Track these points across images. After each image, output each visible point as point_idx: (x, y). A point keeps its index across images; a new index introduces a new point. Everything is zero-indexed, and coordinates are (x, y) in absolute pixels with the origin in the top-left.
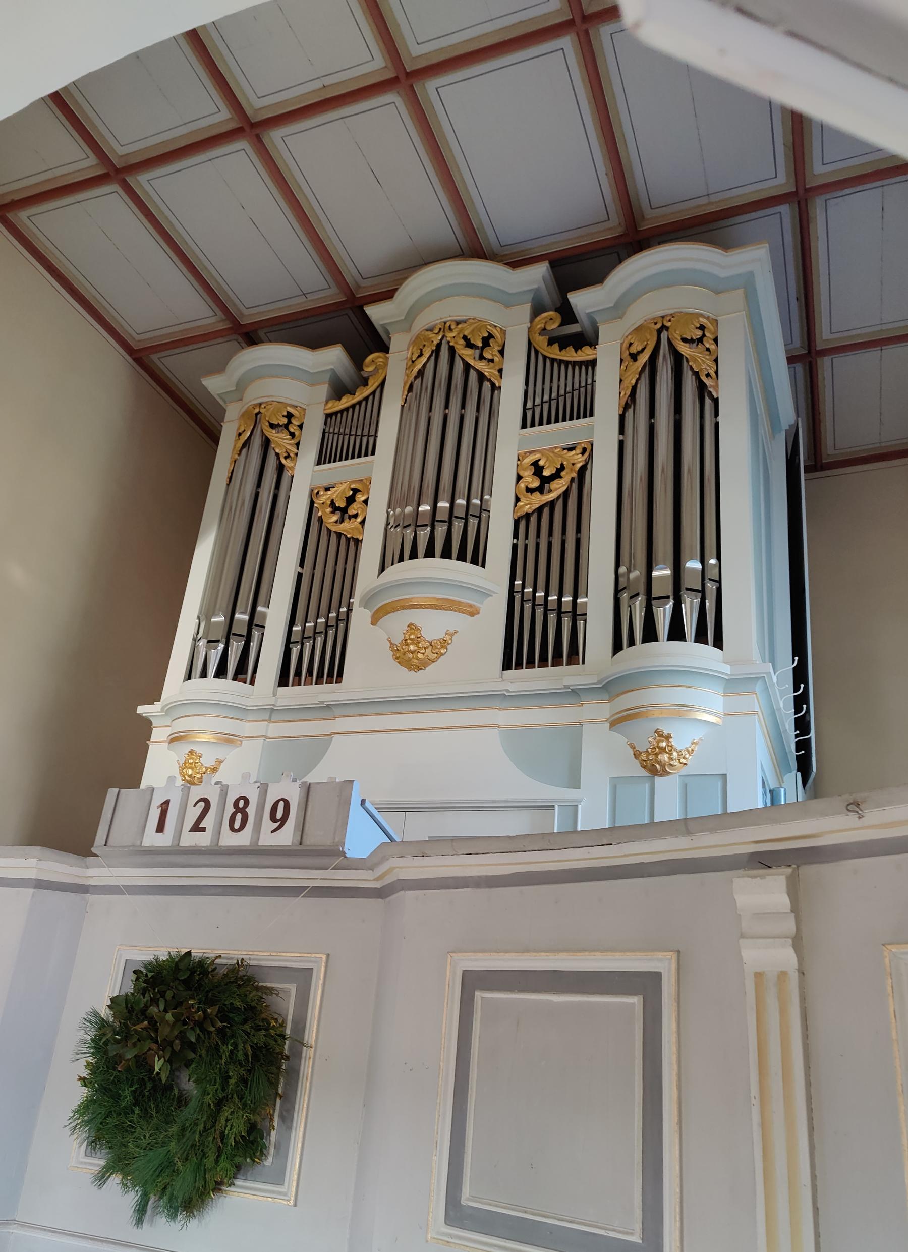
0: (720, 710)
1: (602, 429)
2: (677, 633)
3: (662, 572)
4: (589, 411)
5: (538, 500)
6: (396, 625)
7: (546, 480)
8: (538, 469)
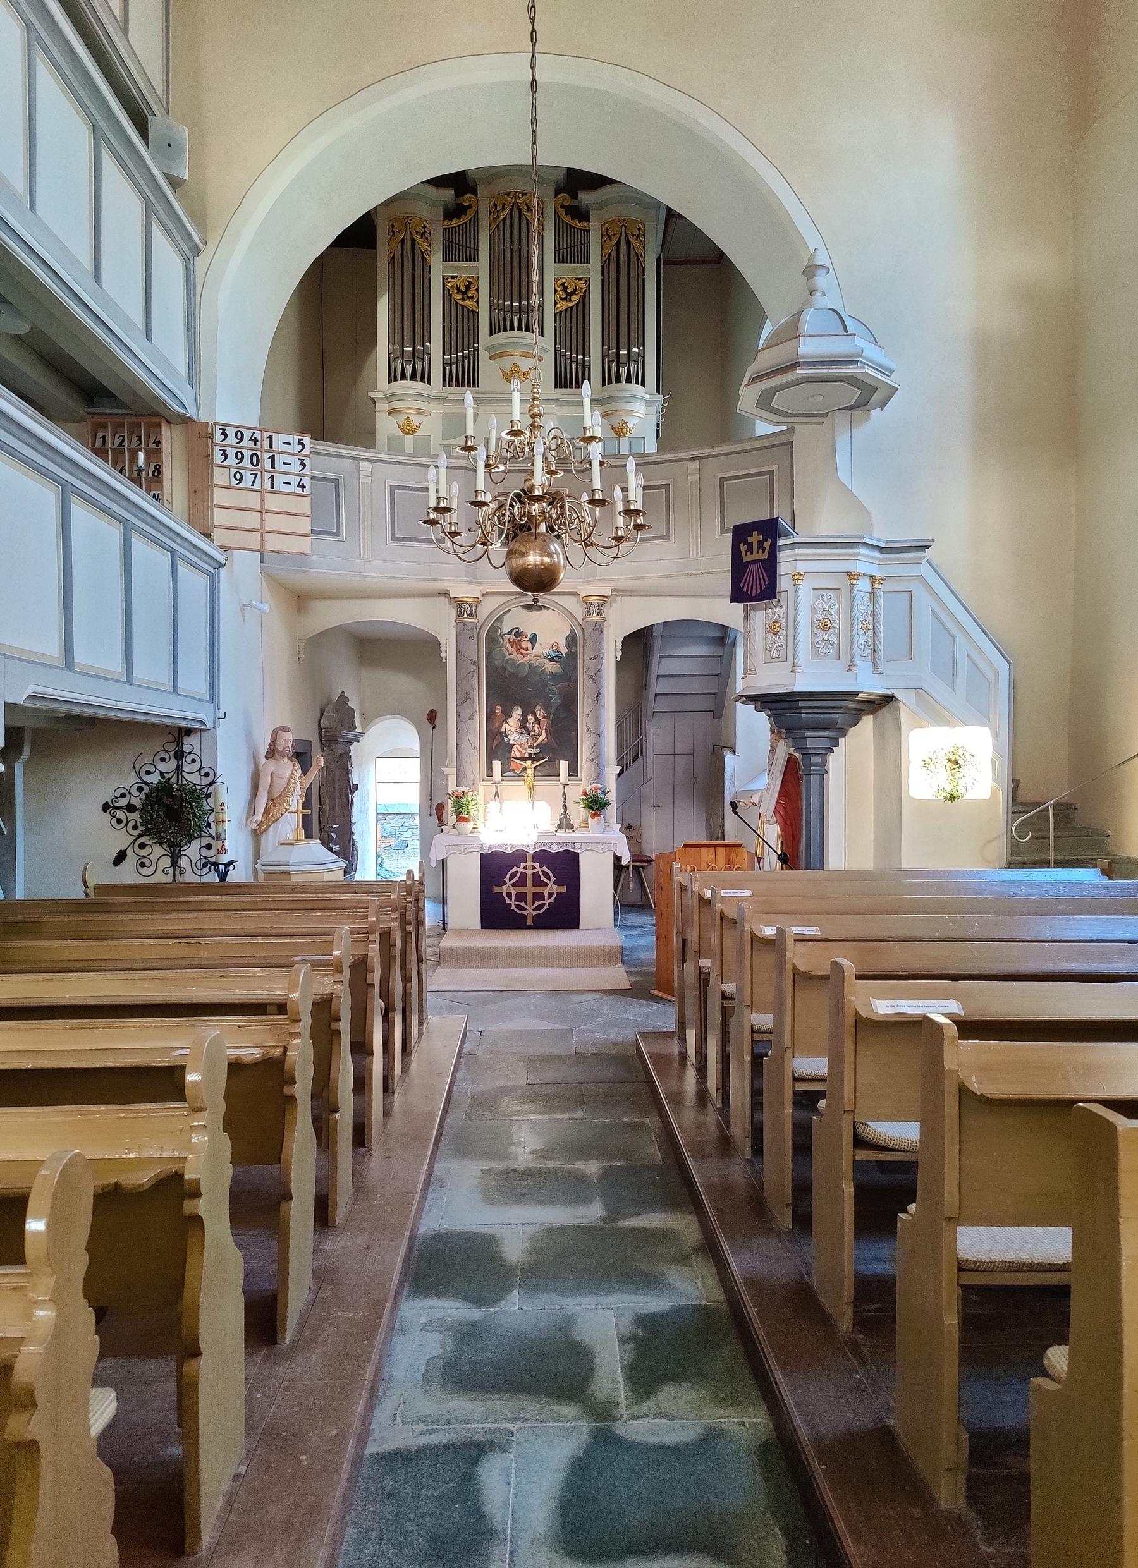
0: (641, 409)
1: (594, 270)
2: (629, 380)
3: (623, 352)
4: (587, 260)
5: (566, 305)
6: (507, 363)
8: (565, 289)
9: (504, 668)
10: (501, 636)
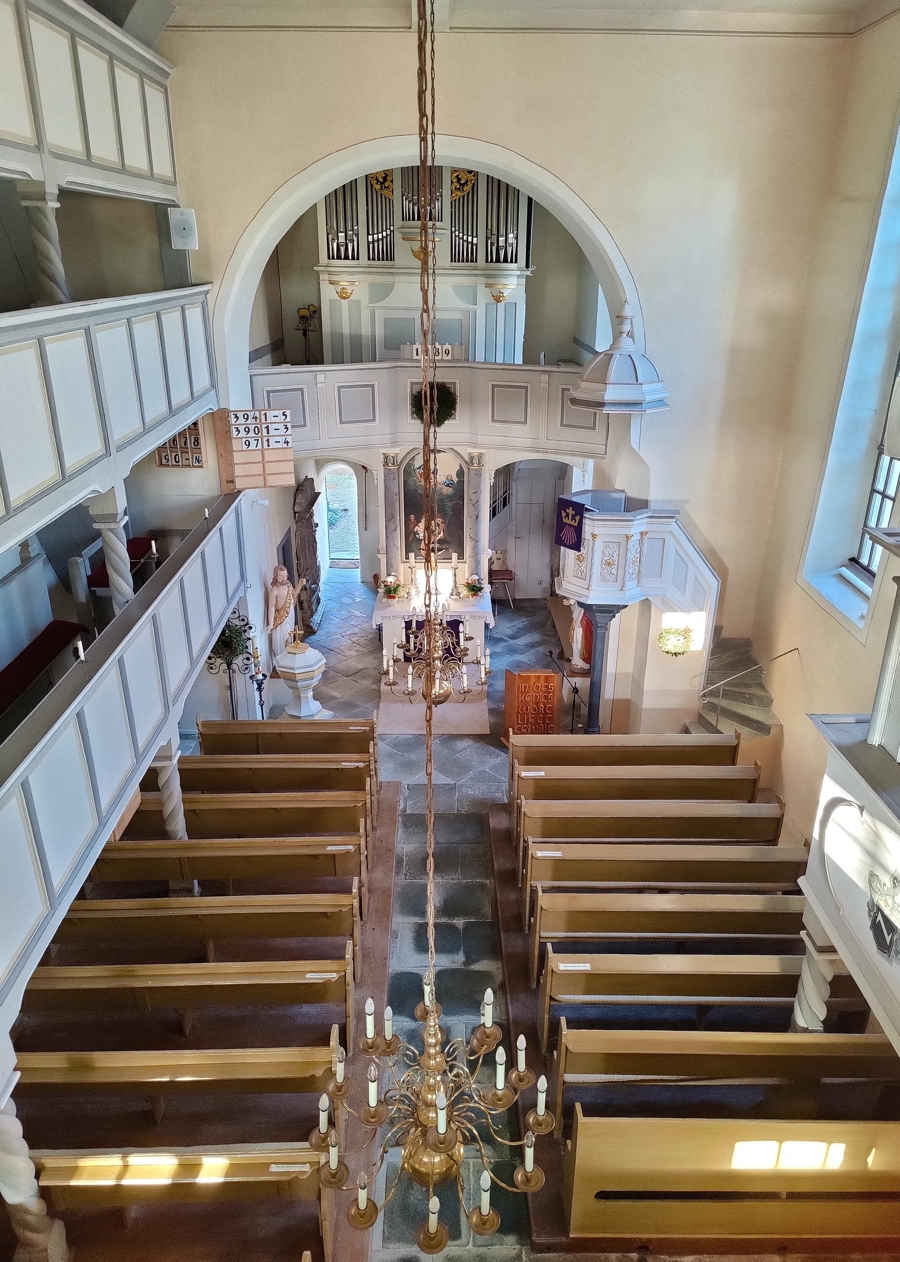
0: (513, 282)
2: (505, 261)
7: (463, 185)
8: (459, 180)
9: (416, 491)
10: (414, 470)
